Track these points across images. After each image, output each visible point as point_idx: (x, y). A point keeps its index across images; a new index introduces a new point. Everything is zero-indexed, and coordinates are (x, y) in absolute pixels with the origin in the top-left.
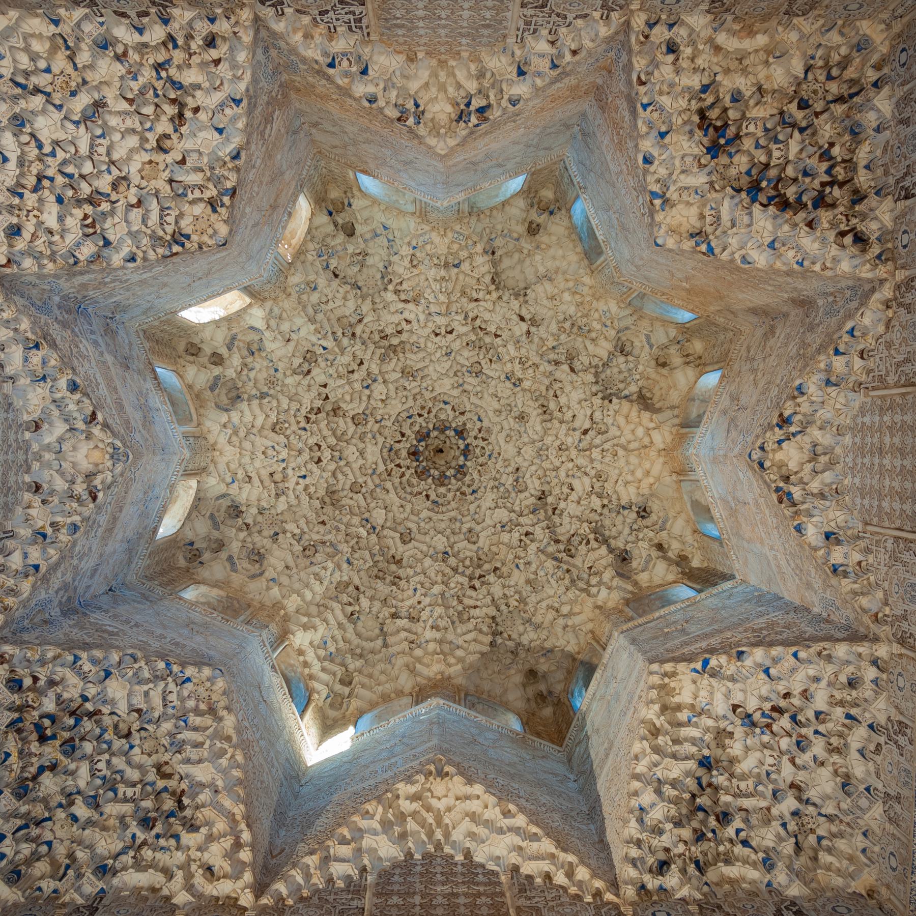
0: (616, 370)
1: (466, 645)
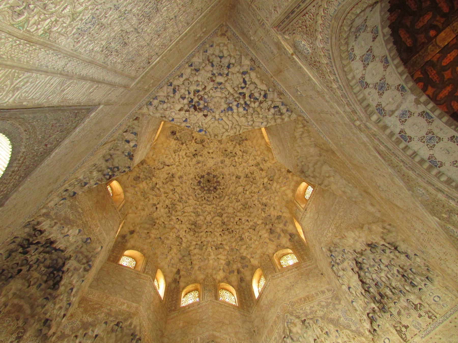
0: (145, 173)
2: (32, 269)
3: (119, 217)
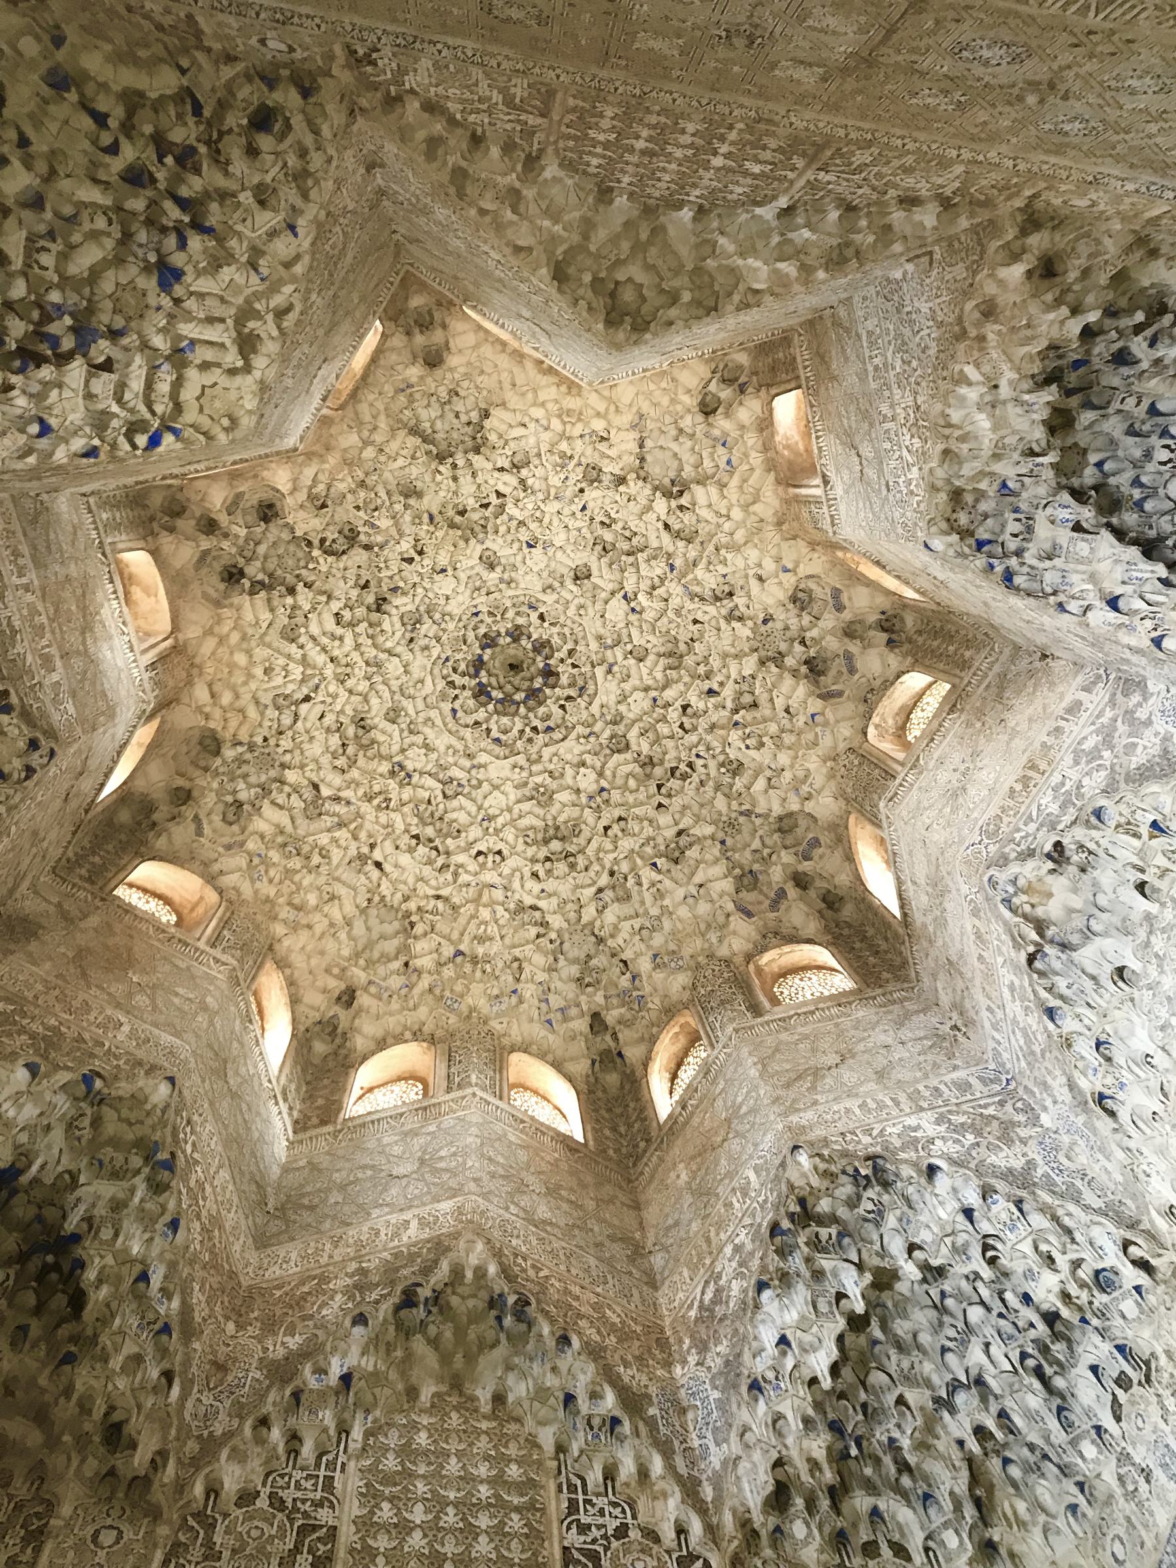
0: (253, 779)
3: (217, 961)
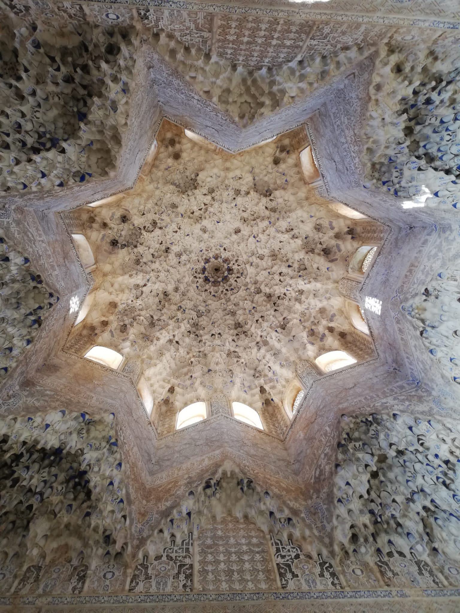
0: (129, 316)
1: (212, 174)
2: (45, 496)
